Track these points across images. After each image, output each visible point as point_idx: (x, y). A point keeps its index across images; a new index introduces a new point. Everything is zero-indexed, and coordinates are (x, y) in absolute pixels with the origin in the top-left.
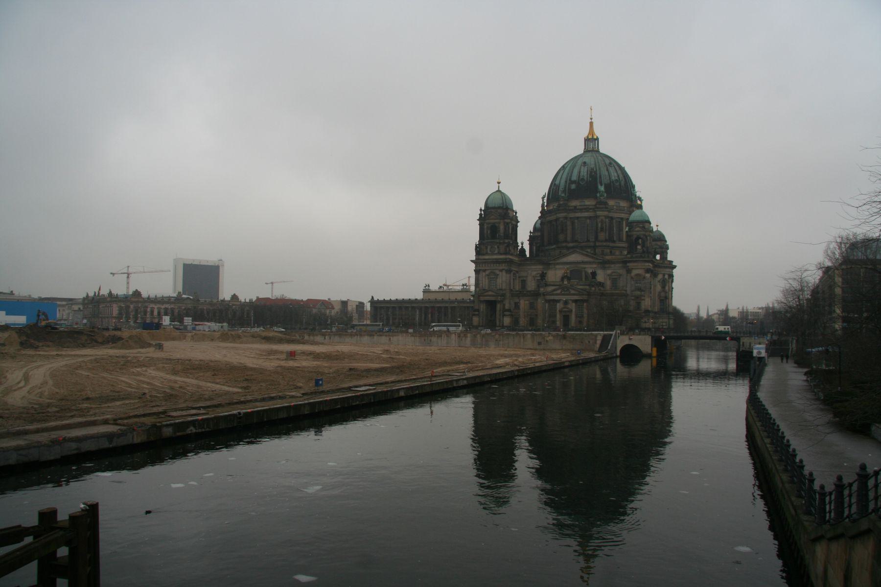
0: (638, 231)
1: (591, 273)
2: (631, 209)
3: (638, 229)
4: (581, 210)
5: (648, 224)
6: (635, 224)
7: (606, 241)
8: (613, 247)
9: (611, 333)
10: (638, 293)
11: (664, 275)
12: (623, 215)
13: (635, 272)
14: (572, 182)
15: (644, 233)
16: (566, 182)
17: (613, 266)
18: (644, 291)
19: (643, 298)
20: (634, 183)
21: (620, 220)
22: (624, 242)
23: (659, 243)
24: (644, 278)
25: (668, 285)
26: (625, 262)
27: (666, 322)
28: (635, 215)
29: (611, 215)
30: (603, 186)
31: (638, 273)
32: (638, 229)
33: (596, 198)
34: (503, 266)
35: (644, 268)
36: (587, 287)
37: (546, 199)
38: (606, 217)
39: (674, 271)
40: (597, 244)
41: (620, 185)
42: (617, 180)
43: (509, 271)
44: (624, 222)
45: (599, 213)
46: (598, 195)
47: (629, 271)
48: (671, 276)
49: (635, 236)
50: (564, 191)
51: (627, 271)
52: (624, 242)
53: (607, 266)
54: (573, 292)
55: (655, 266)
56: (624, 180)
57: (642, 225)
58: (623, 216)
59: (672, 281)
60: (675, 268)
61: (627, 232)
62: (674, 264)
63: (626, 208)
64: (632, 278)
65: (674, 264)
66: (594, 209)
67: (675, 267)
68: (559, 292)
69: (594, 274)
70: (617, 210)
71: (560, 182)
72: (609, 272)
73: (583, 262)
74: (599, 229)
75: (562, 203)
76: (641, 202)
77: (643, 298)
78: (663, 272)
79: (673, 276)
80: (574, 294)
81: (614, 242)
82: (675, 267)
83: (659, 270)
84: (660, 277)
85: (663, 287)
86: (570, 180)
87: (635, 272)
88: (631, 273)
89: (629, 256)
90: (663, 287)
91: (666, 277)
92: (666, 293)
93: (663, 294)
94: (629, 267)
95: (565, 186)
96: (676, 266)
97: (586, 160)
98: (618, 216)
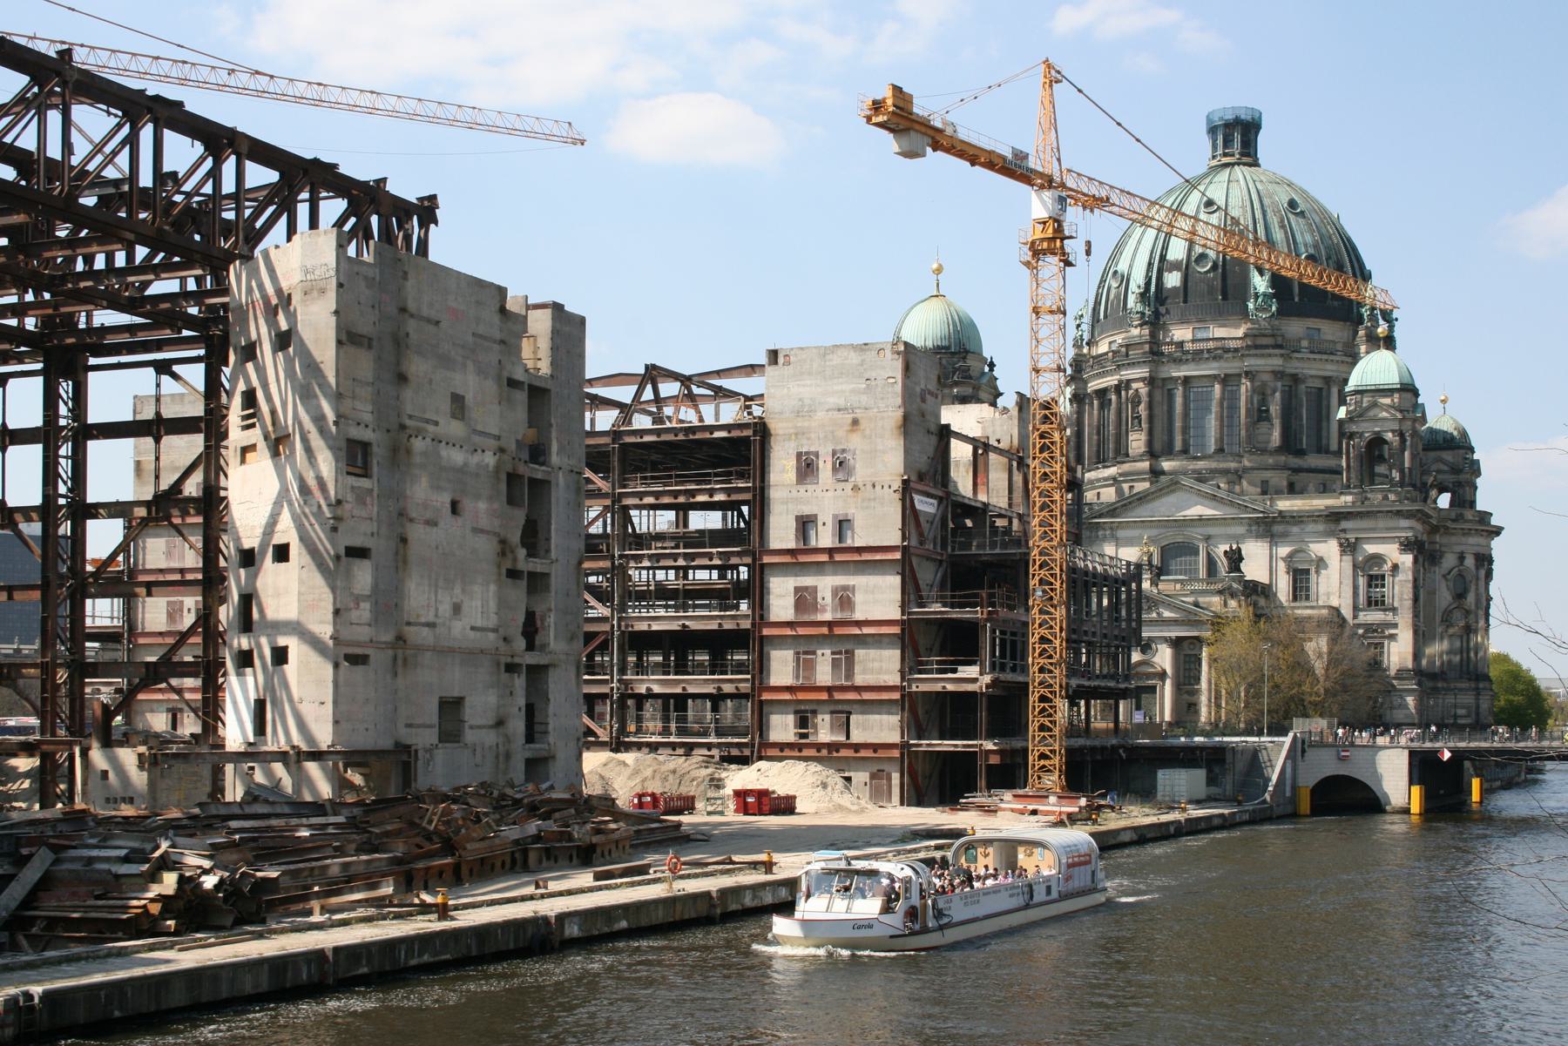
1: (1226, 552)
4: (1197, 356)
8: (1297, 471)
9: (1281, 739)
10: (1374, 617)
11: (1461, 558)
12: (1329, 367)
14: (1176, 266)
16: (1150, 264)
17: (1295, 529)
19: (1393, 631)
20: (229, 125)
23: (1448, 456)
25: (1473, 588)
27: (1467, 707)
28: (1374, 369)
29: (1294, 367)
30: (1267, 277)
33: (1244, 313)
36: (1216, 599)
37: (1087, 319)
38: (1278, 374)
44: (1335, 391)
46: (1251, 306)
48: (1485, 561)
50: (1144, 296)
51: (1341, 545)
53: (1277, 528)
55: (1434, 530)
58: (1330, 369)
59: (1489, 575)
61: (1341, 422)
62: (1494, 521)
65: (1494, 521)
66: (1236, 350)
67: (1497, 531)
69: (1235, 559)
70: (1312, 352)
71: (1131, 266)
75: (1136, 332)
76: (1391, 328)
78: (1459, 549)
79: (1491, 561)
80: (1175, 622)
81: (1300, 453)
82: (1497, 531)
83: (1445, 540)
84: (1449, 561)
85: (1460, 596)
86: (1163, 258)
90: (1460, 596)
91: (1470, 562)
95: (1148, 284)
97: (1217, 192)
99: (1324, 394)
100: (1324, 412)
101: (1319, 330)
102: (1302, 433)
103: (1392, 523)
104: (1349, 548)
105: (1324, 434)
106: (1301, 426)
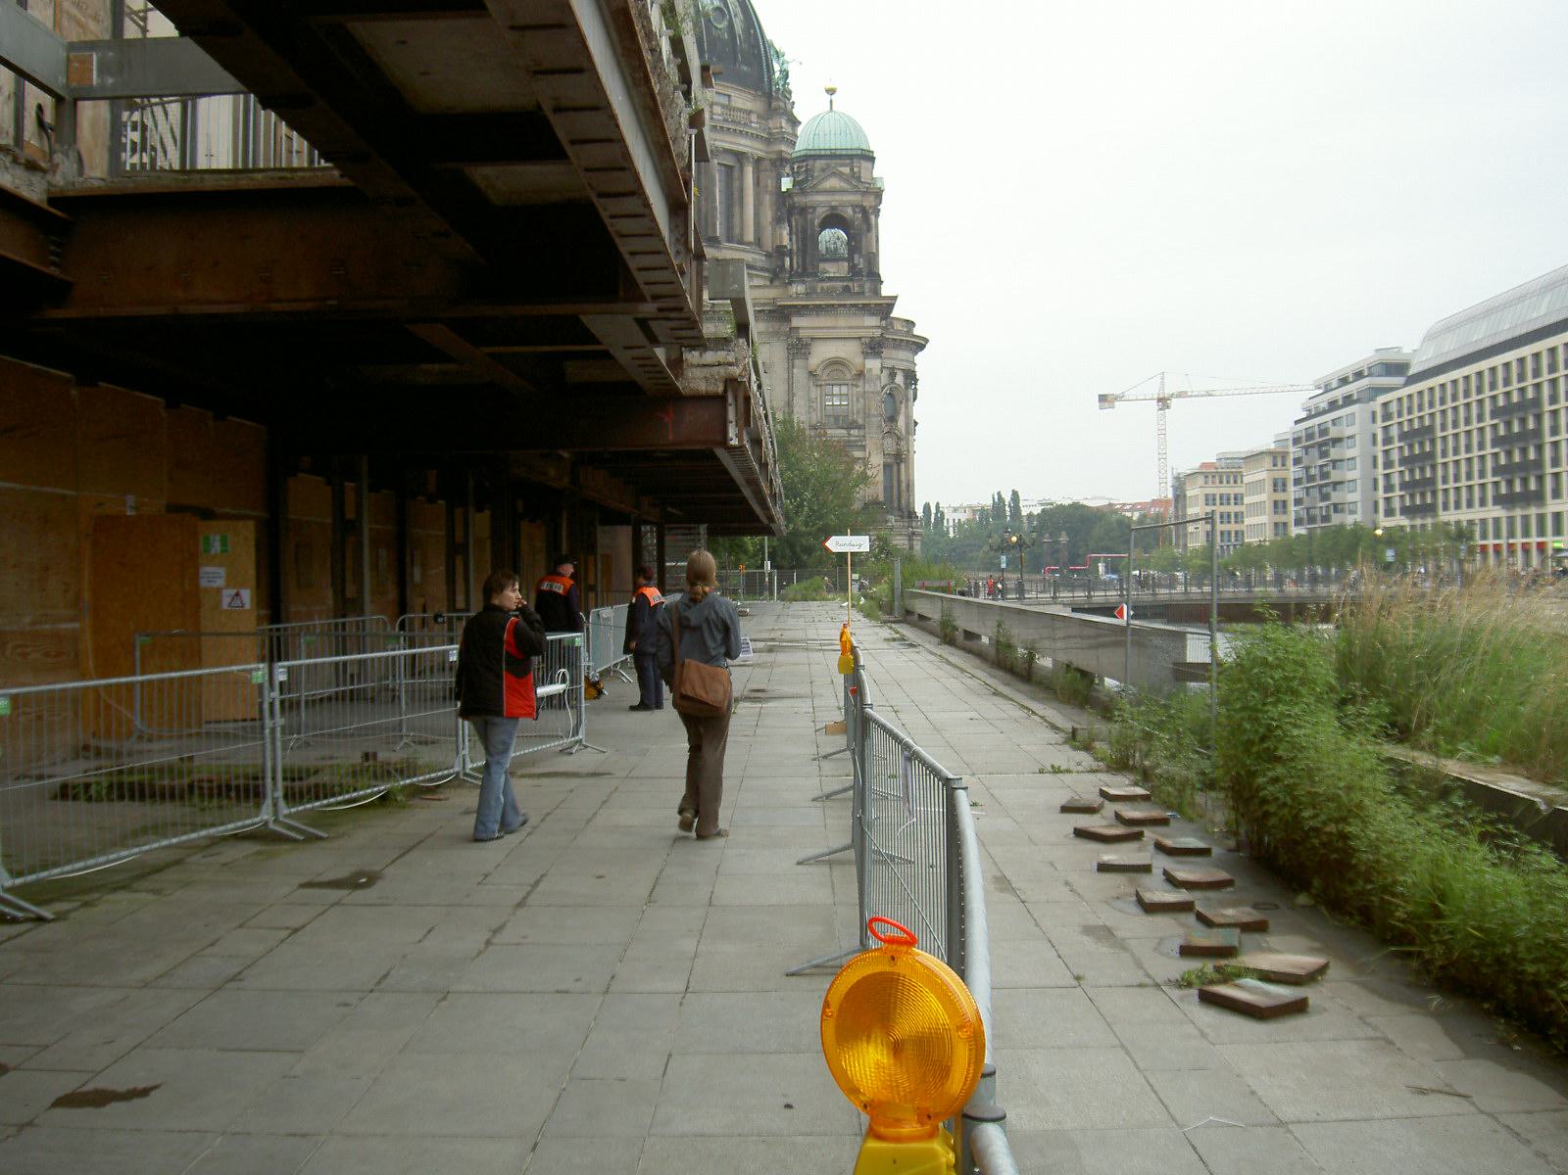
0: (832, 191)
2: (771, 124)
3: (833, 183)
5: (864, 164)
6: (819, 164)
11: (892, 375)
12: (743, 141)
13: (822, 353)
15: (855, 198)
18: (859, 427)
19: (857, 454)
21: (729, 161)
22: (749, 244)
24: (861, 374)
25: (903, 410)
26: (781, 314)
31: (842, 355)
32: (833, 183)
35: (860, 338)
39: (921, 359)
41: (731, 26)
42: (718, 9)
44: (749, 171)
47: (799, 348)
48: (911, 377)
49: (821, 212)
52: (749, 244)
56: (741, 15)
57: (846, 170)
60: (921, 347)
62: (917, 331)
63: (754, 118)
64: (811, 374)
65: (917, 331)
67: (920, 345)
70: (725, 120)
77: (857, 454)
82: (920, 345)
87: (822, 353)
88: (806, 356)
89: (798, 288)
91: (899, 379)
92: (899, 438)
94: (802, 333)
96: (927, 341)
98: (727, 146)
99: (736, 174)
100: (736, 195)
101: (729, 96)
102: (714, 217)
103: (855, 321)
104: (799, 348)
105: (736, 220)
106: (715, 208)
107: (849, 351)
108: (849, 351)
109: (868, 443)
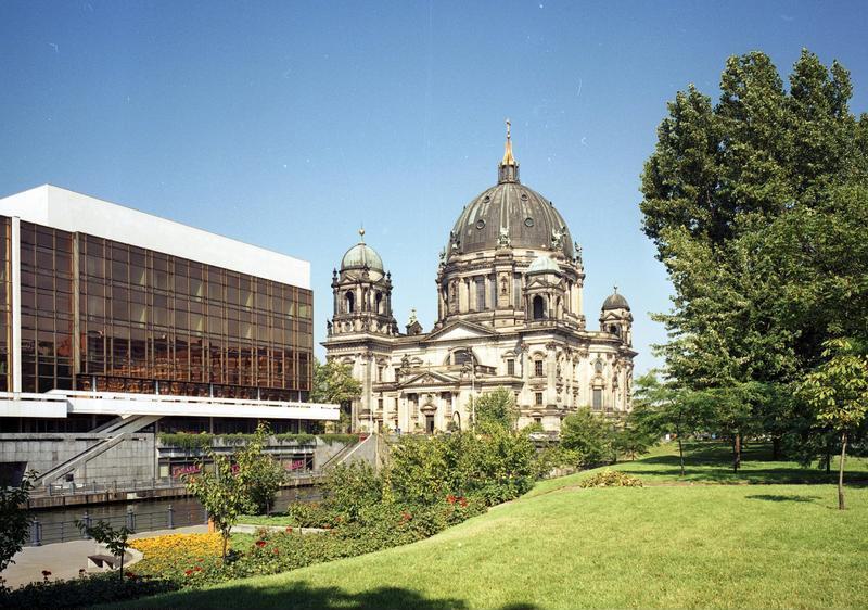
7: (510, 307)
23: (618, 312)
29: (517, 269)
32: (537, 284)
34: (362, 350)
40: (497, 313)
43: (369, 357)
45: (498, 268)
54: (436, 381)
57: (541, 279)
68: (419, 382)
72: (503, 351)
73: (468, 339)
74: (500, 292)
84: (593, 356)
87: (533, 349)
90: (599, 372)
91: (604, 356)
93: (598, 382)
107: (542, 348)
108: (542, 348)
109: (550, 383)
